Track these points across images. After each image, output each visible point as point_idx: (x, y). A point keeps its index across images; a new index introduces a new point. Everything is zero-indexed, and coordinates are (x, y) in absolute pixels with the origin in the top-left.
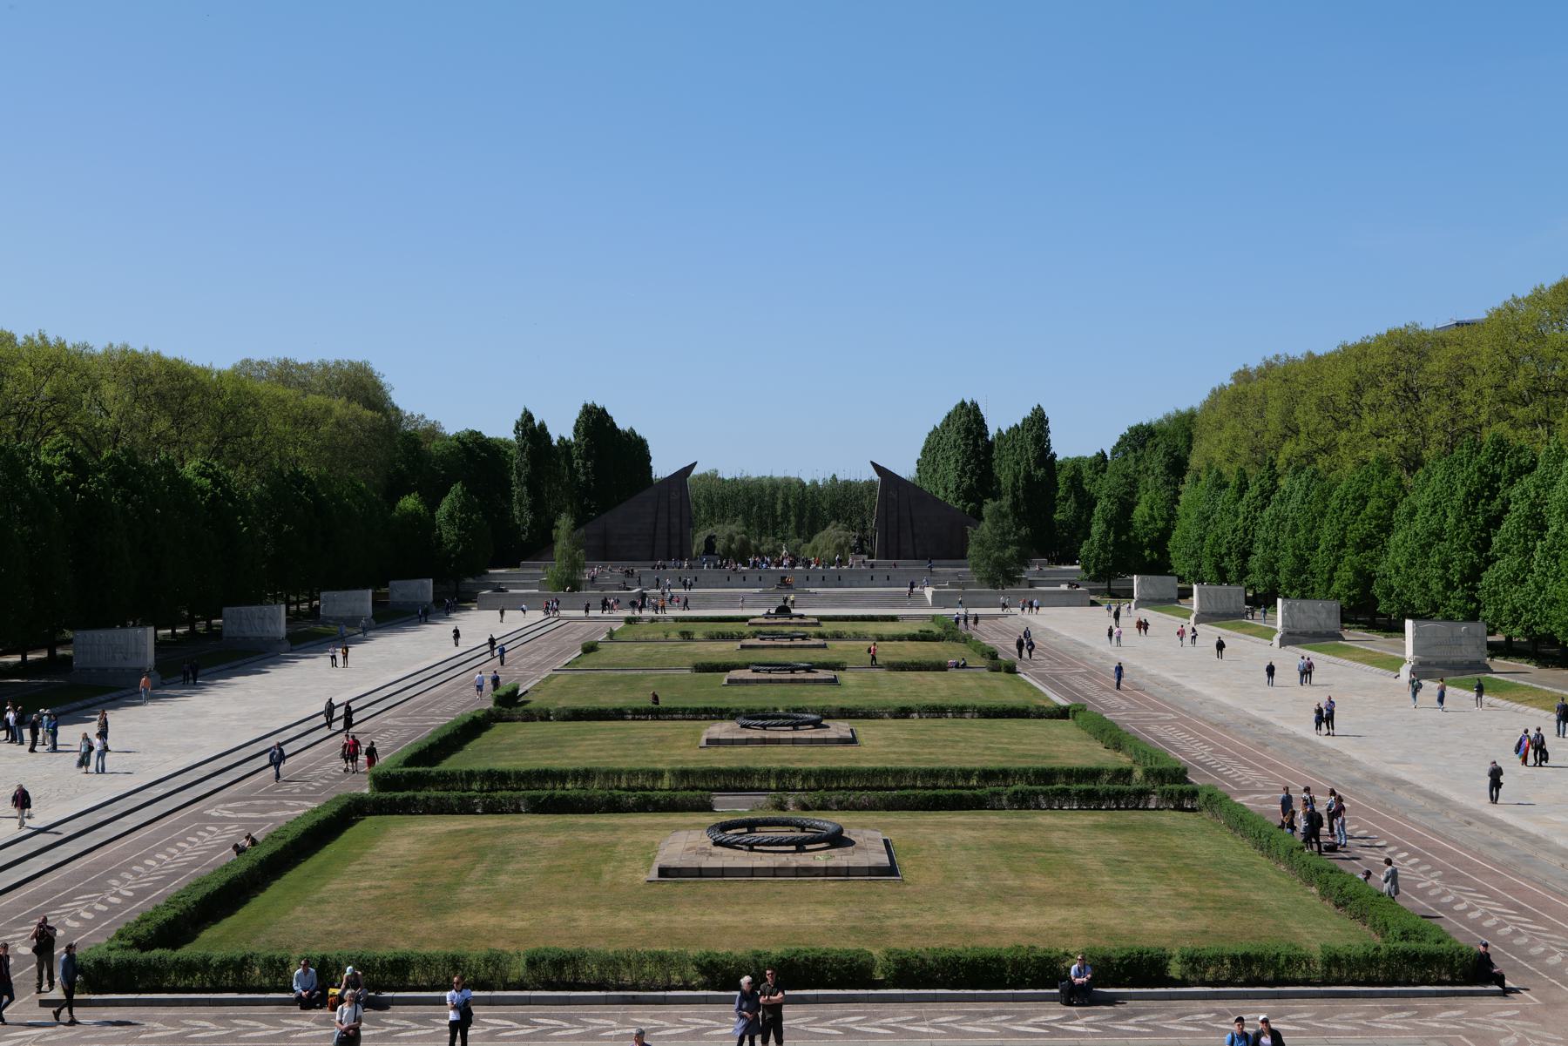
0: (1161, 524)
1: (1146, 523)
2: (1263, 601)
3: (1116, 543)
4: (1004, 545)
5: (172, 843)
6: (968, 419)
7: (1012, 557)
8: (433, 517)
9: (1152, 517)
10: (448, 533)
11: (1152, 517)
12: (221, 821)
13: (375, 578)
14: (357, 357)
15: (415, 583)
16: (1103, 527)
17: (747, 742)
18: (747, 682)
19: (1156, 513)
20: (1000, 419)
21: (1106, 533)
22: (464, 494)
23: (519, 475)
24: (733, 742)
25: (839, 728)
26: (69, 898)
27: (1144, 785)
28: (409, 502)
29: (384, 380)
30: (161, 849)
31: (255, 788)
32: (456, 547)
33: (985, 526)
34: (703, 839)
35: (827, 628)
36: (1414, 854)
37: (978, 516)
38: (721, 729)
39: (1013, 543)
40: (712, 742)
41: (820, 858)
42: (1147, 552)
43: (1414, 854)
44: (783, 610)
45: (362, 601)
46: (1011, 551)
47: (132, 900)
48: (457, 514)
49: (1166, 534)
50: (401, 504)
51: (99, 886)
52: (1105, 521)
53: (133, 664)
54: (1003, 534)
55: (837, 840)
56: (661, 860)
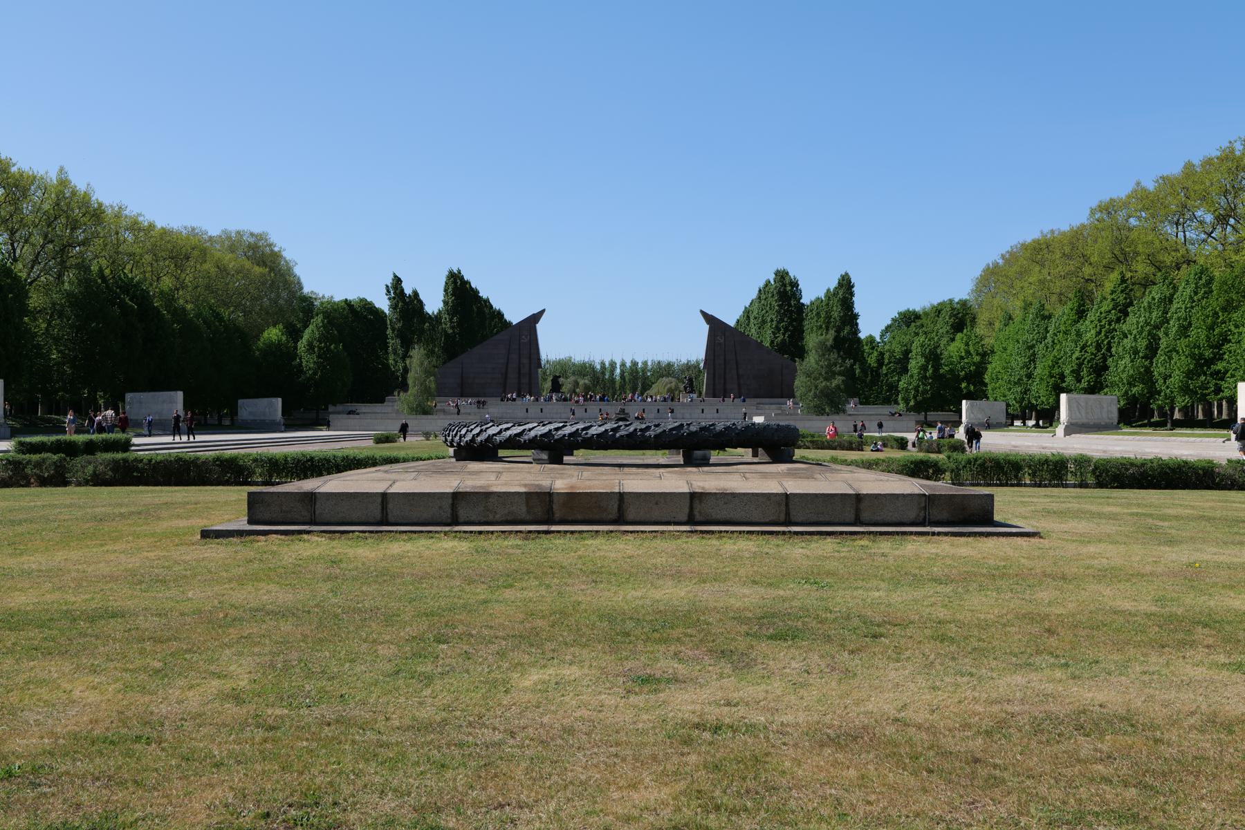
0: (977, 359)
1: (962, 358)
3: (937, 376)
4: (830, 375)
6: (784, 290)
7: (838, 387)
8: (296, 348)
9: (968, 352)
10: (308, 361)
11: (968, 352)
14: (257, 230)
15: (264, 402)
16: (922, 361)
19: (971, 349)
20: (812, 291)
21: (924, 368)
22: (324, 326)
23: (393, 329)
28: (273, 334)
29: (287, 255)
32: (315, 373)
33: (811, 360)
37: (801, 353)
39: (840, 374)
42: (963, 385)
46: (838, 381)
48: (316, 343)
49: (981, 368)
50: (265, 334)
52: (923, 355)
54: (829, 366)
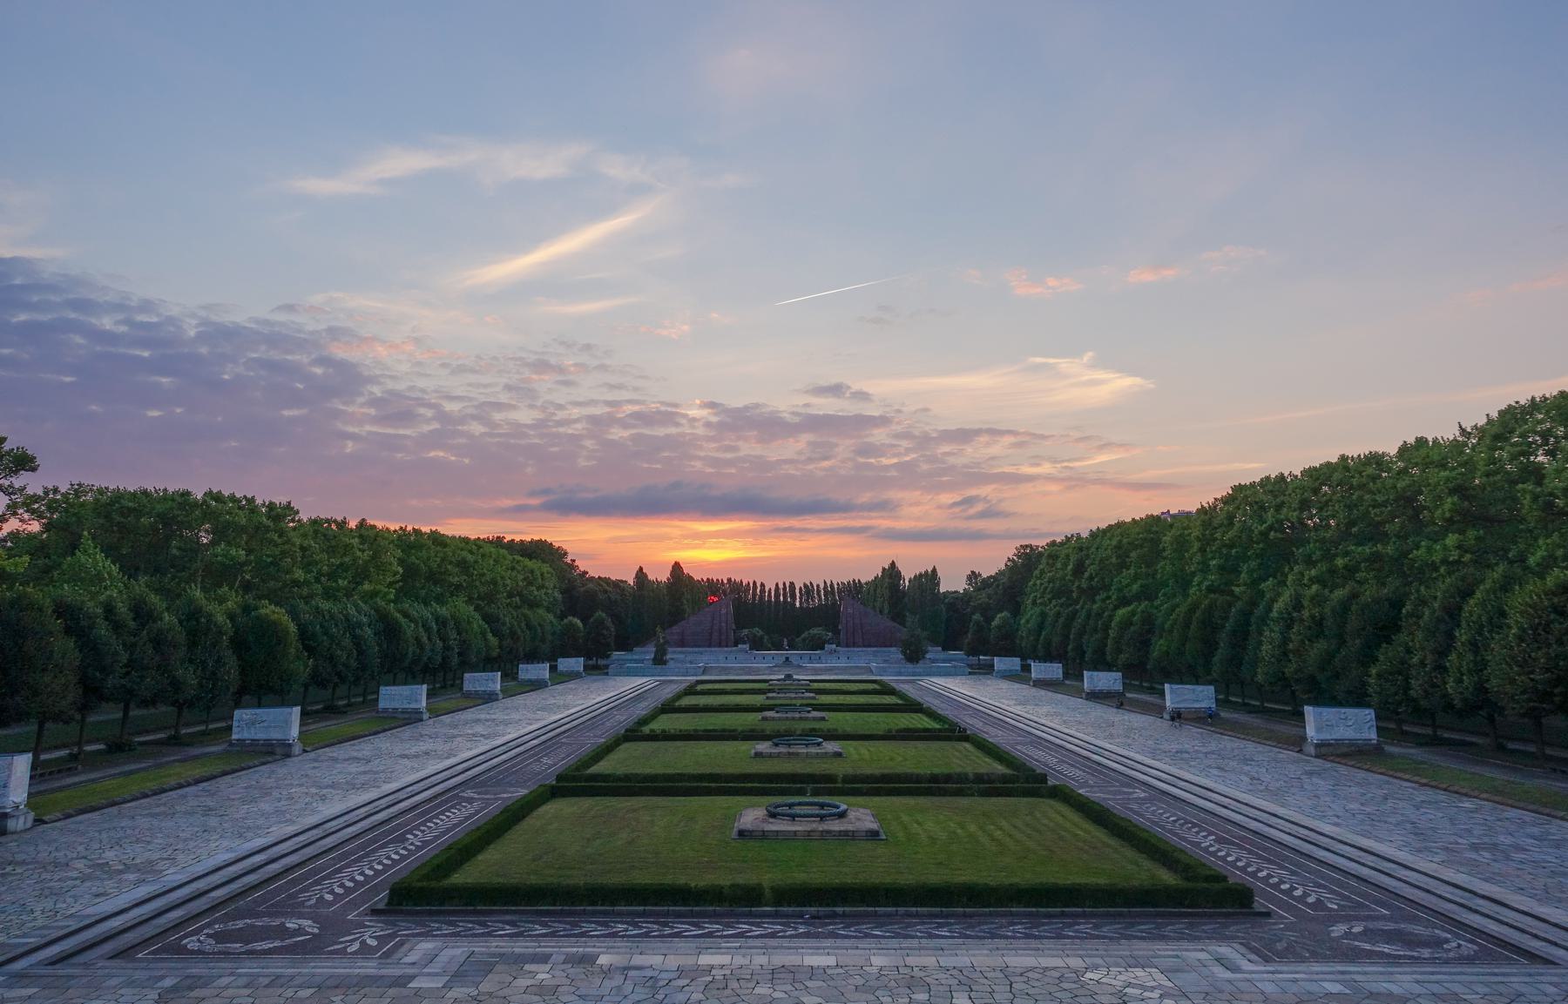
2: (1073, 673)
5: (442, 813)
12: (470, 800)
13: (552, 658)
15: (572, 661)
17: (779, 755)
18: (773, 719)
24: (770, 756)
25: (831, 747)
26: (382, 847)
27: (1021, 781)
30: (436, 817)
31: (491, 778)
34: (760, 812)
35: (816, 685)
36: (1195, 825)
38: (763, 747)
40: (758, 755)
41: (836, 826)
43: (1195, 825)
44: (789, 677)
45: (541, 671)
47: (419, 848)
51: (402, 839)
53: (413, 706)
55: (842, 815)
56: (738, 826)
